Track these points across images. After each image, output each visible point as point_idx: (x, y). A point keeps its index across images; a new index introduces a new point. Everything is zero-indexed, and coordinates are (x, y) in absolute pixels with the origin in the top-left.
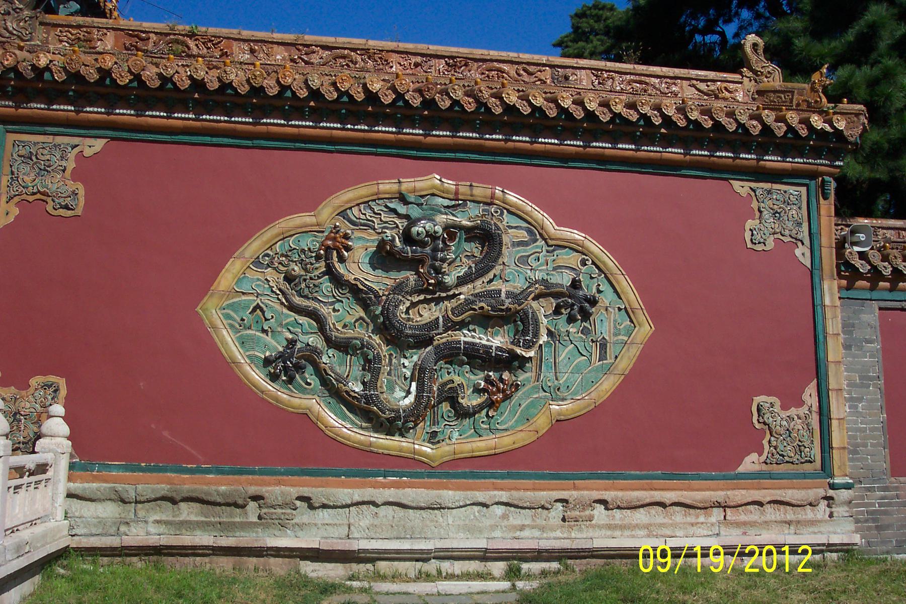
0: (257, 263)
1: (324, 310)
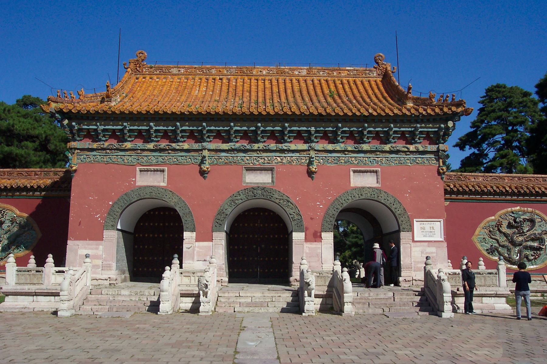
0: (483, 228)
1: (499, 238)
